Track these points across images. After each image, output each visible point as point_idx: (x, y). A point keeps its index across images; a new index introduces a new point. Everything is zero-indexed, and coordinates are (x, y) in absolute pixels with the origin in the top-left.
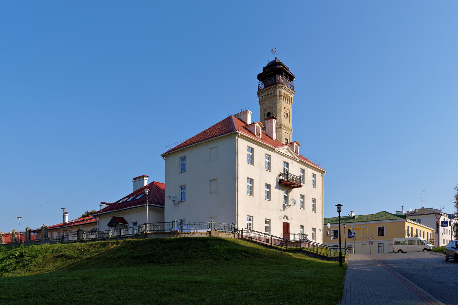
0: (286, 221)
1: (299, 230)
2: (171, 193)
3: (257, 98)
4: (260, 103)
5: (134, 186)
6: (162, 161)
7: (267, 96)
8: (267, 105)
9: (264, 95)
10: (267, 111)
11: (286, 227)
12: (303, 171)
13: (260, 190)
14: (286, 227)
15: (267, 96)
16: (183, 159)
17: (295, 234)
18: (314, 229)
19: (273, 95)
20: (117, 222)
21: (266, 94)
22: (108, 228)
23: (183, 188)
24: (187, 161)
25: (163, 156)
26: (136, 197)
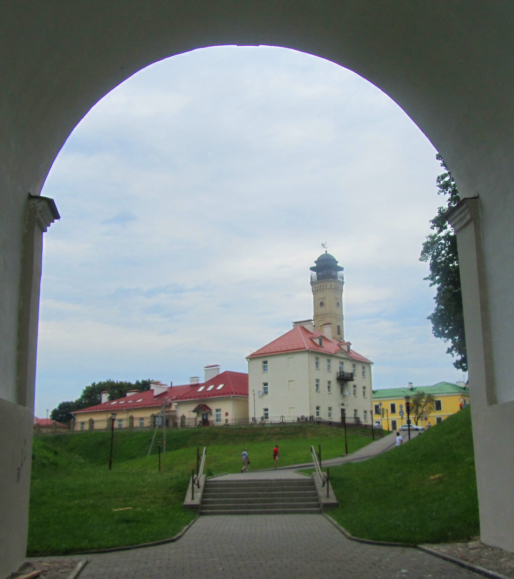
0: (343, 407)
1: (352, 415)
2: (254, 386)
3: (310, 287)
4: (313, 292)
5: (206, 377)
6: (246, 362)
7: (319, 288)
8: (320, 295)
9: (316, 286)
10: (320, 301)
11: (343, 411)
12: (354, 366)
13: (323, 386)
14: (343, 411)
15: (319, 288)
16: (265, 362)
17: (351, 418)
18: (365, 412)
19: (325, 287)
20: (202, 409)
21: (319, 285)
22: (194, 415)
23: (266, 384)
24: (268, 364)
25: (247, 358)
26: (216, 386)
